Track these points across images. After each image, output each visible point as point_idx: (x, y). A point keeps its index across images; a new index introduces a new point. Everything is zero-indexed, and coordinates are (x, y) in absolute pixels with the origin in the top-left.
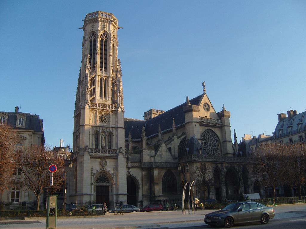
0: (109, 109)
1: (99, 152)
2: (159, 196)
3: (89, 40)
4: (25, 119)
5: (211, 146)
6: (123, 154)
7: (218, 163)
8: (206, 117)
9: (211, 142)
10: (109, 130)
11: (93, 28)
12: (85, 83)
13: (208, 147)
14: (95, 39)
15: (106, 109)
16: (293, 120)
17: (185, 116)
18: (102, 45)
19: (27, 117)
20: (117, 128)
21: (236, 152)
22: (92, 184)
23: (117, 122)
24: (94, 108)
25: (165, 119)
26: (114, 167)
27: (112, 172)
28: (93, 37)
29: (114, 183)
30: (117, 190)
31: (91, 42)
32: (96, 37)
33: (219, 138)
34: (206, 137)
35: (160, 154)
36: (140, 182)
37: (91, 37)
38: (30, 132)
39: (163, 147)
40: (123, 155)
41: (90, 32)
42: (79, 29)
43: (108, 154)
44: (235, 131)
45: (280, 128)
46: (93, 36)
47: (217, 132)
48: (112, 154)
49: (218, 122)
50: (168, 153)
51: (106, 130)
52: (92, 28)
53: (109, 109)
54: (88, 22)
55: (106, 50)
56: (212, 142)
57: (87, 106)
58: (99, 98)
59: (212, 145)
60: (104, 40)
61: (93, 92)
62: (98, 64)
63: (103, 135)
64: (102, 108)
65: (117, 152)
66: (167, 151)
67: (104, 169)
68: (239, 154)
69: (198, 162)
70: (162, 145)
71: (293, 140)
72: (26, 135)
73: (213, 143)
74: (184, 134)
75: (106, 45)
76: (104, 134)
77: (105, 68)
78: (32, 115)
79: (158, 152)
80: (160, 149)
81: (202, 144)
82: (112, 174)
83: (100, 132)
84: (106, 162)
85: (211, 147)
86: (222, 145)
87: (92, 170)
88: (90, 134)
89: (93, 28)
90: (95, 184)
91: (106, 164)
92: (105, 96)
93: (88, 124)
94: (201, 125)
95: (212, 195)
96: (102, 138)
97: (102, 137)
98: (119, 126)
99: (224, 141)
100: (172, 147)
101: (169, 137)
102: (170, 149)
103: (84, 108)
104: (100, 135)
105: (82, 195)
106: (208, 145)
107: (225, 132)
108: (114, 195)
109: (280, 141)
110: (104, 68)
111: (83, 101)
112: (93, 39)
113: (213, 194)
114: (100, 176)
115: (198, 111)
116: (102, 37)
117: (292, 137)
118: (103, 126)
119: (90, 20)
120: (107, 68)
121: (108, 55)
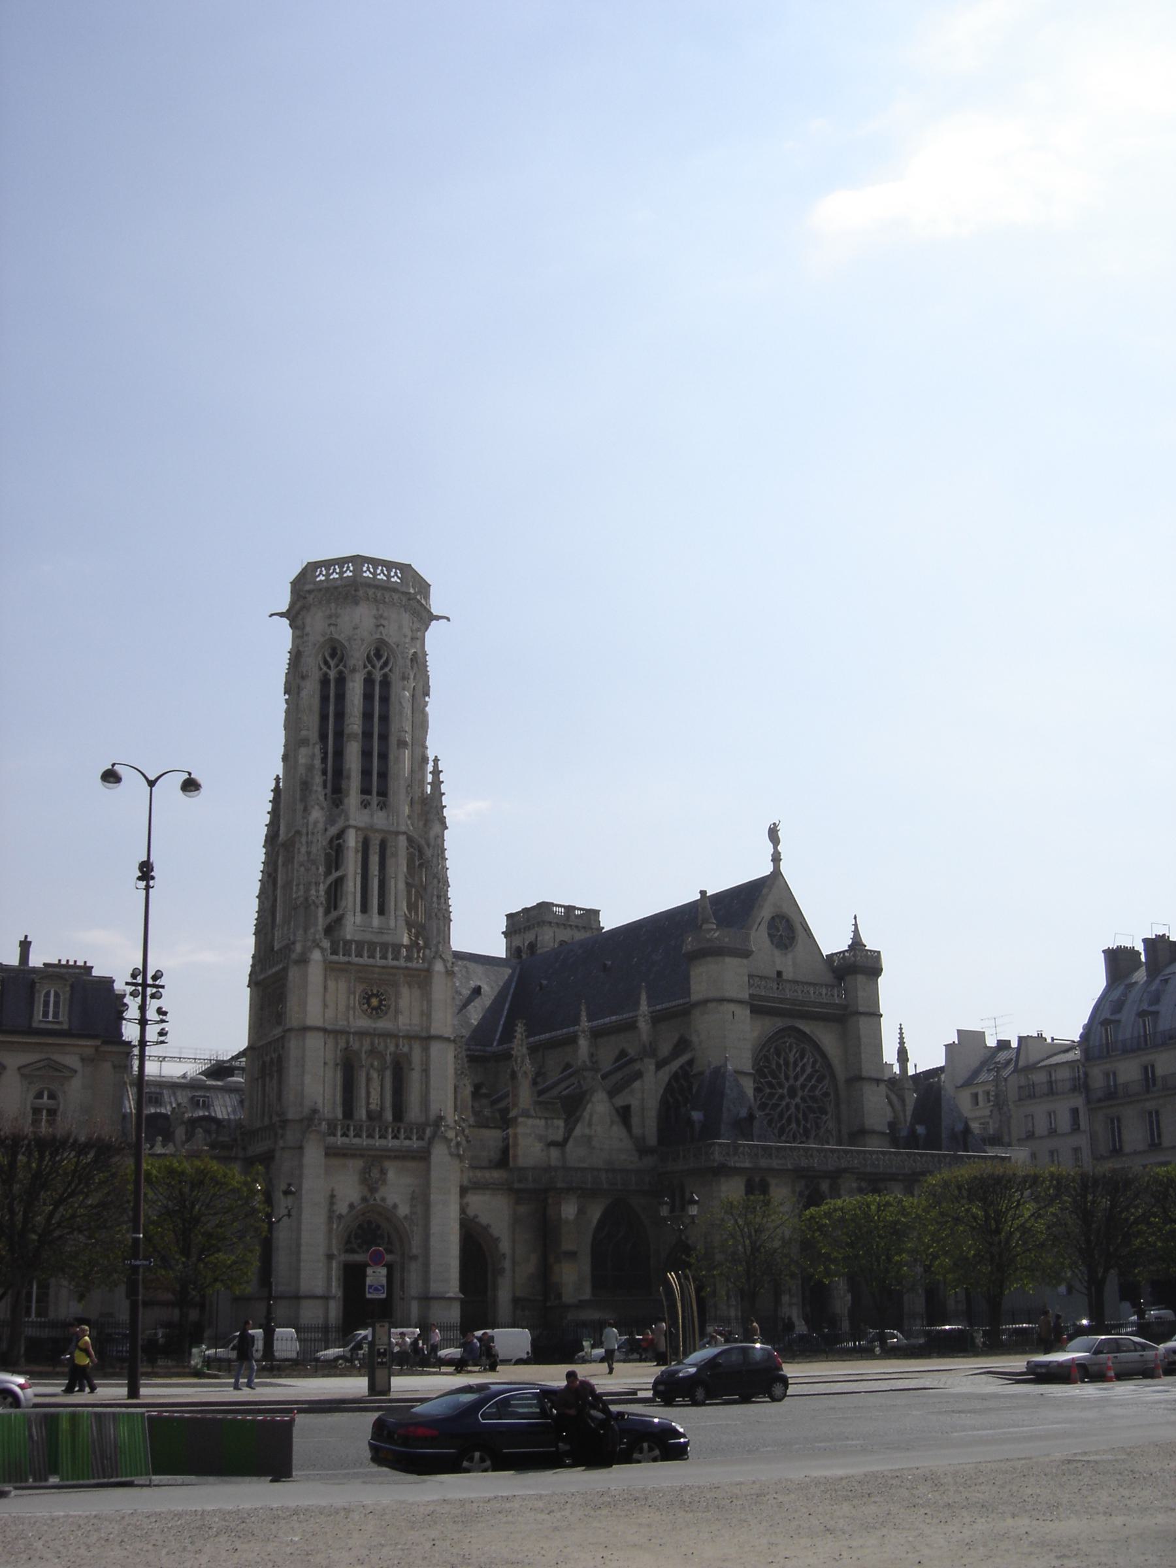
0: (395, 963)
1: (357, 1135)
2: (581, 1305)
3: (315, 676)
4: (68, 996)
5: (798, 1100)
6: (447, 1141)
9: (799, 1083)
10: (397, 1046)
11: (336, 625)
12: (306, 858)
13: (784, 1103)
14: (341, 673)
15: (383, 962)
16: (1166, 981)
17: (692, 973)
18: (368, 697)
19: (72, 987)
20: (427, 1039)
21: (905, 1121)
22: (330, 1257)
23: (427, 1015)
24: (341, 958)
25: (605, 965)
26: (414, 1191)
27: (403, 1210)
28: (332, 663)
29: (415, 1251)
30: (426, 1279)
31: (325, 682)
32: (345, 666)
33: (829, 1066)
34: (778, 1065)
35: (587, 1131)
36: (505, 1246)
38: (88, 1045)
39: (599, 1107)
40: (449, 1147)
41: (322, 640)
42: (272, 615)
43: (391, 1143)
44: (901, 1034)
45: (1108, 1016)
46: (333, 655)
47: (827, 1039)
48: (407, 1143)
50: (618, 1131)
51: (386, 1047)
52: (330, 625)
53: (395, 963)
54: (312, 596)
55: (385, 719)
56: (801, 1080)
57: (316, 955)
58: (359, 918)
59: (800, 1094)
60: (378, 676)
61: (335, 892)
62: (354, 784)
63: (372, 1065)
64: (371, 961)
65: (424, 1133)
66: (612, 1123)
67: (375, 1200)
68: (912, 1132)
69: (737, 1171)
70: (594, 1099)
71: (1159, 1072)
72: (72, 1061)
73: (803, 1086)
74: (683, 1045)
75: (385, 700)
76: (376, 1063)
77: (383, 793)
78: (71, 963)
79: (579, 1125)
80: (586, 1115)
81: (757, 1090)
82: (406, 1217)
83: (363, 1056)
84: (383, 1172)
85: (797, 1106)
87: (332, 1204)
88: (325, 1063)
89: (332, 628)
90: (345, 1257)
91: (384, 1182)
92: (382, 911)
93: (319, 1023)
94: (758, 1008)
95: (790, 1305)
96: (369, 1080)
97: (368, 1074)
98: (433, 1032)
100: (635, 1103)
101: (623, 1053)
102: (624, 1114)
103: (303, 961)
104: (362, 1066)
105: (297, 1298)
106: (782, 1097)
107: (859, 1038)
108: (413, 1298)
109: (1107, 1075)
110: (379, 794)
111: (300, 932)
113: (794, 1300)
114: (360, 1226)
115: (746, 954)
116: (370, 668)
118: (375, 1029)
120: (391, 793)
121: (393, 740)
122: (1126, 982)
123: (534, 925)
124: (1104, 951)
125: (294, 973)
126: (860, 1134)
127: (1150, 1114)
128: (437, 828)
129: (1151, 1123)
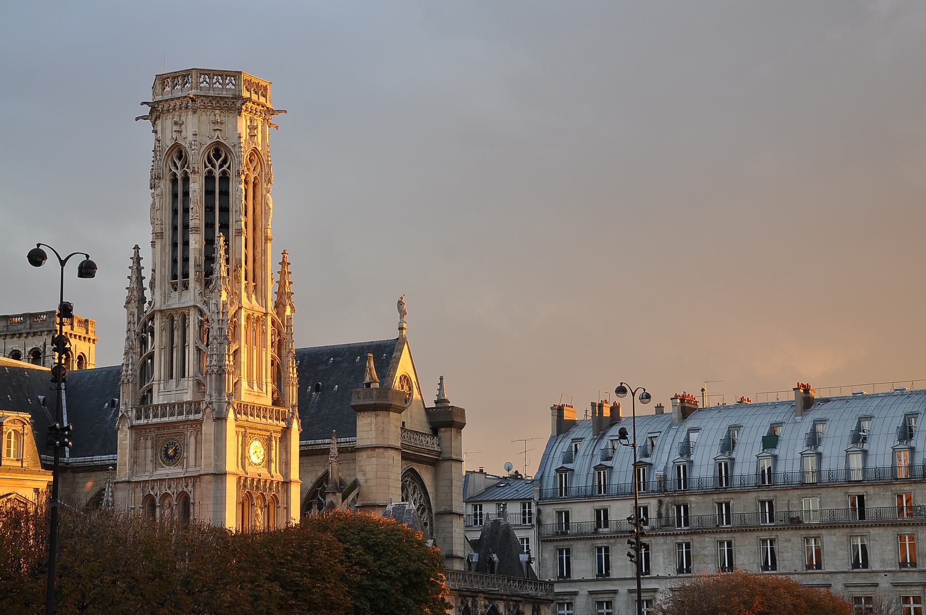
7: (468, 596)
8: (403, 423)
31: (209, 178)
32: (229, 168)
37: (210, 161)
49: (430, 444)
57: (231, 415)
71: (612, 517)
86: (434, 524)
89: (218, 133)
94: (405, 457)
96: (257, 515)
99: (442, 509)
109: (559, 513)
112: (217, 173)
117: (605, 504)
119: (208, 97)
122: (573, 436)
123: (42, 332)
124: (552, 408)
125: (208, 428)
126: (451, 557)
127: (600, 549)
128: (288, 312)
129: (600, 558)
